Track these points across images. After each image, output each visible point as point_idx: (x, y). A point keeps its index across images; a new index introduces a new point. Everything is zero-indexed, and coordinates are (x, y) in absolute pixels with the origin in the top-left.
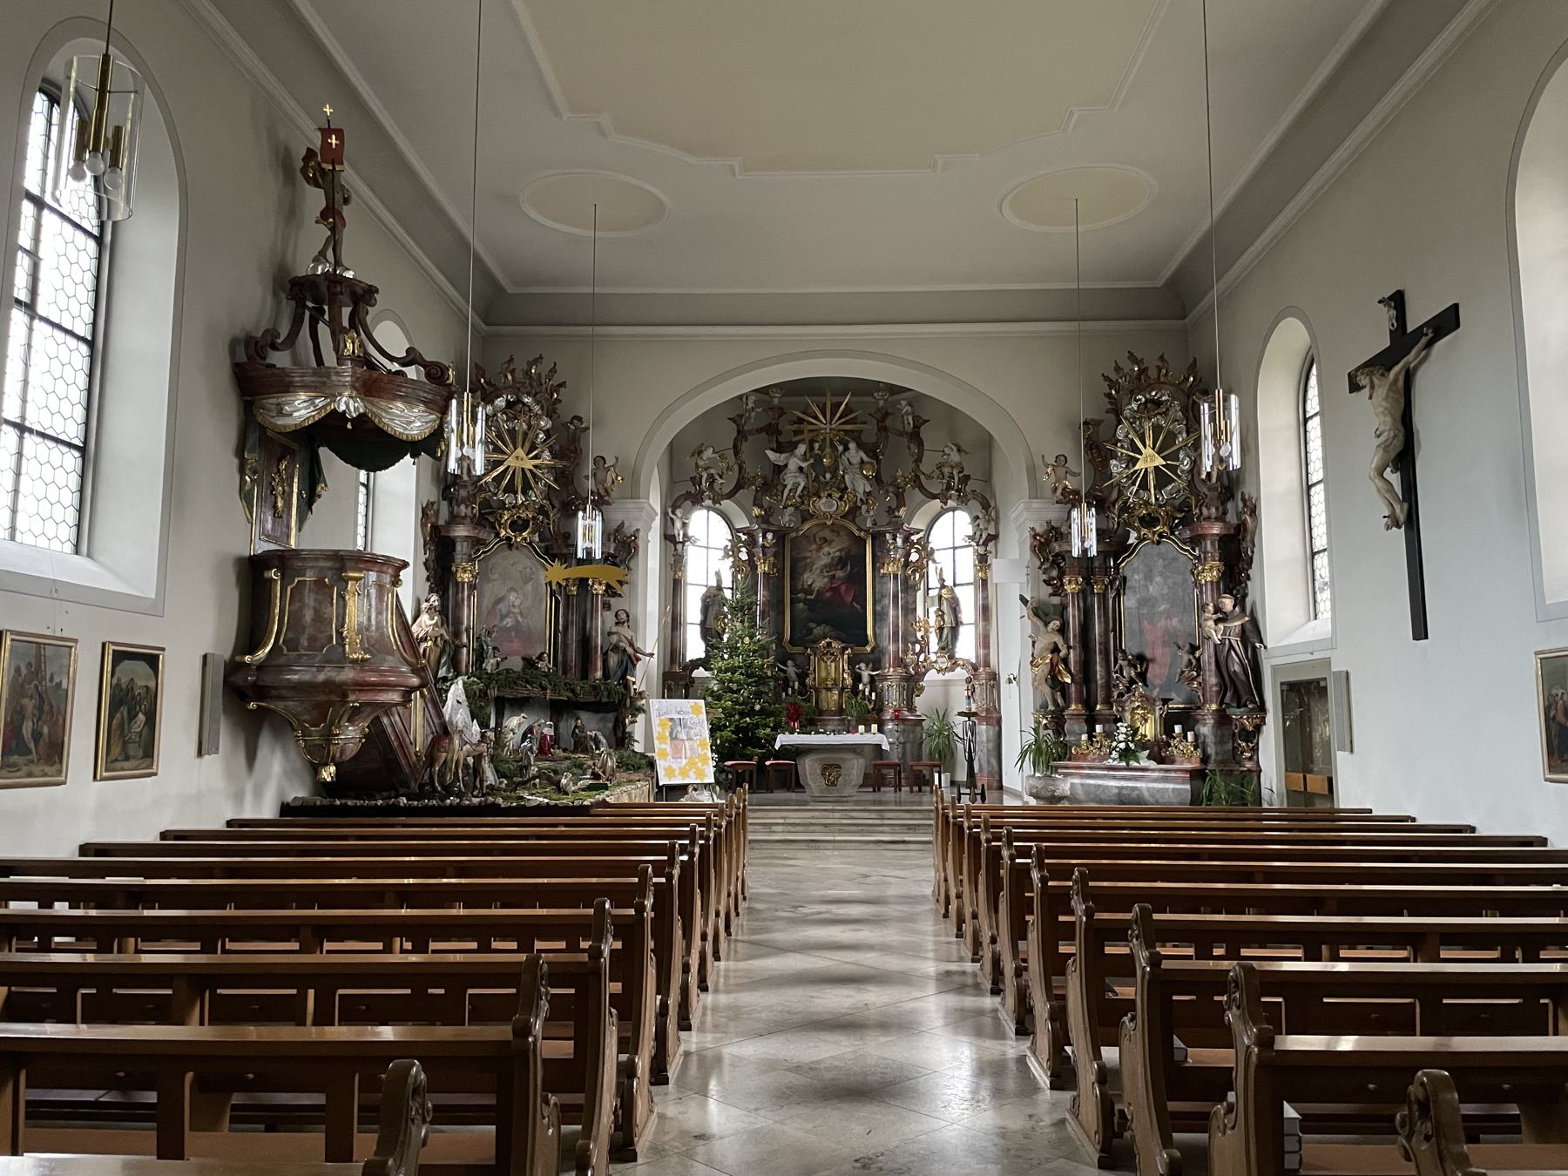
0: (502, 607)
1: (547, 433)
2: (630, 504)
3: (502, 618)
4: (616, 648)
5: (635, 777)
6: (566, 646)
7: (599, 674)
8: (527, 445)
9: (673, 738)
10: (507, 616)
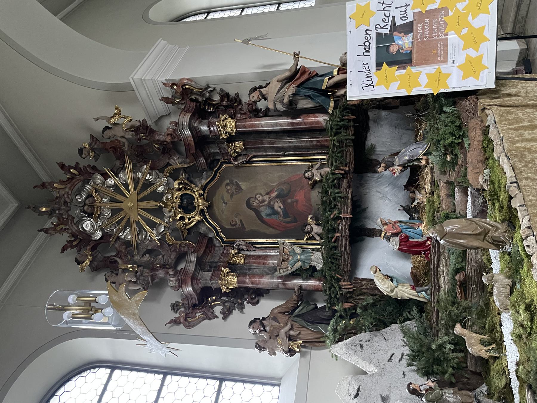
0: (265, 212)
1: (105, 176)
2: (142, 94)
3: (275, 213)
4: (292, 103)
5: (475, 137)
6: (296, 148)
7: (322, 119)
8: (119, 197)
9: (403, 60)
10: (272, 208)
